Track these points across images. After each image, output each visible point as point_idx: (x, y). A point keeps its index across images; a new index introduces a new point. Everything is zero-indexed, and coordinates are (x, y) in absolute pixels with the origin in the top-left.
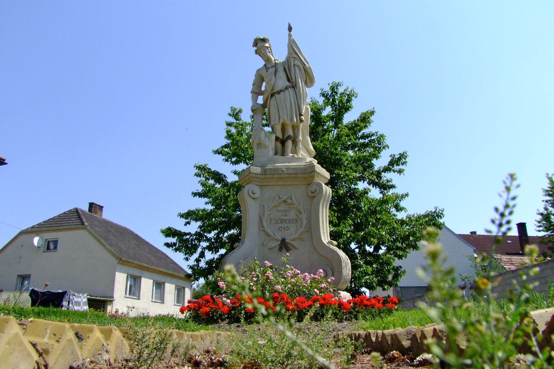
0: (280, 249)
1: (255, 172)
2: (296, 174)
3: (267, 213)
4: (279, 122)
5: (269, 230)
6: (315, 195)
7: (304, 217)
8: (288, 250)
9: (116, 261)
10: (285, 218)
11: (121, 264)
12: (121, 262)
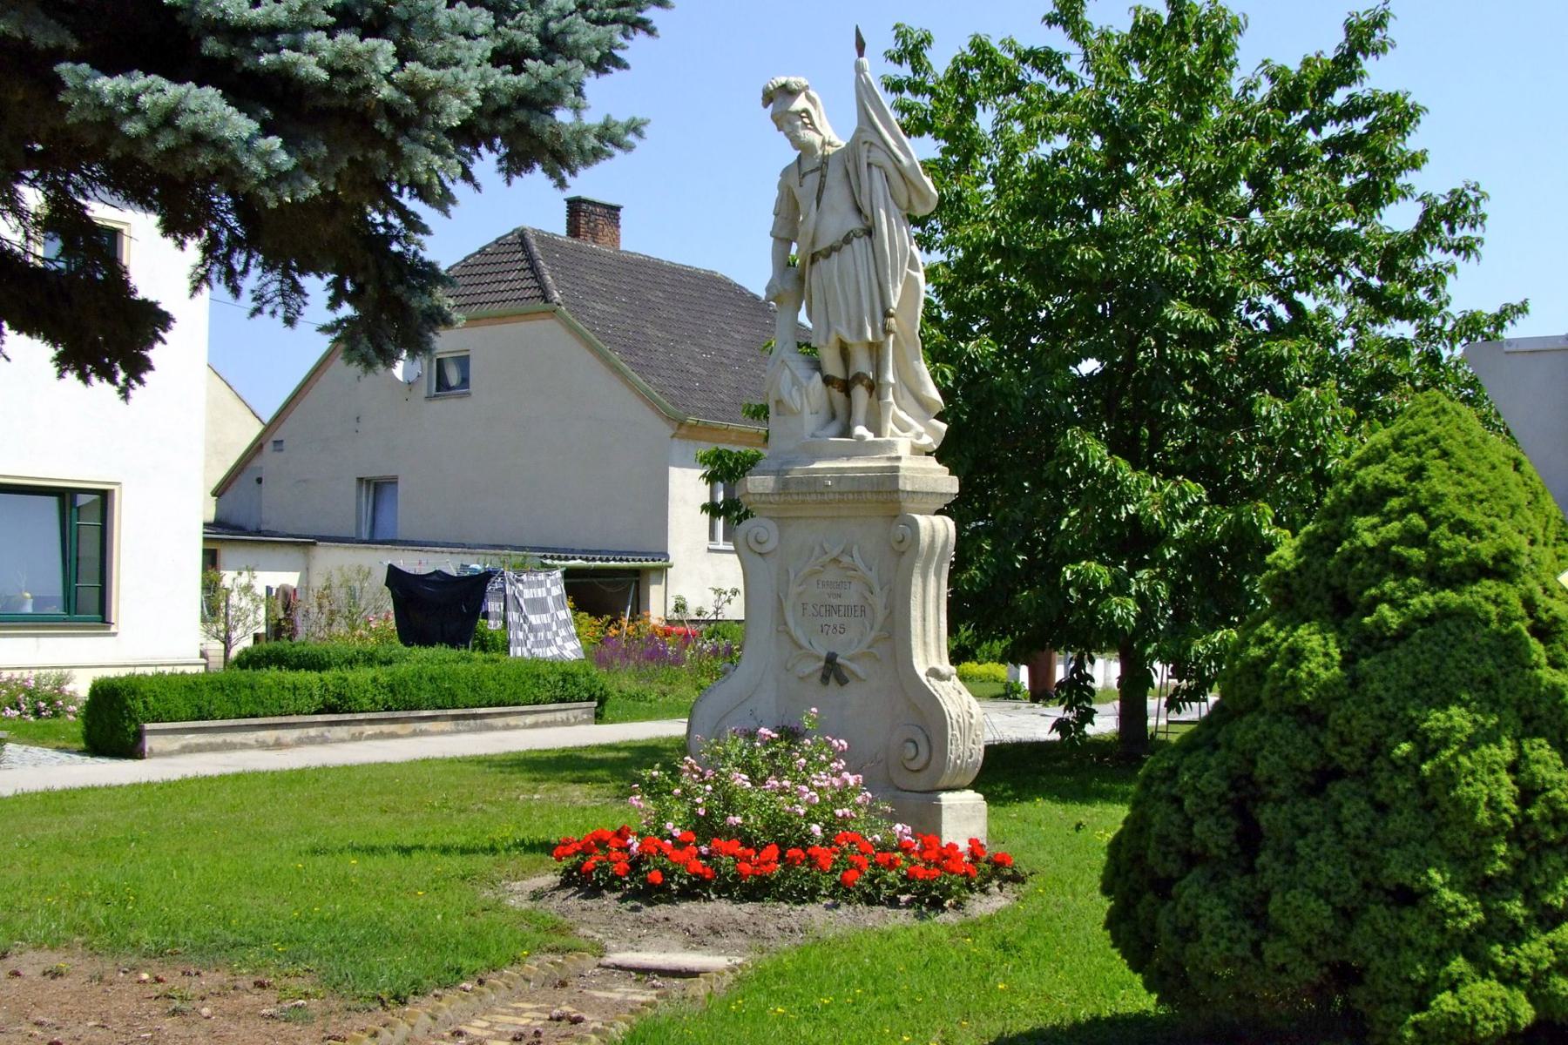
0: (825, 679)
1: (761, 490)
2: (859, 493)
3: (794, 589)
4: (827, 341)
5: (798, 633)
6: (904, 547)
7: (879, 601)
8: (842, 681)
9: (667, 430)
10: (835, 602)
11: (683, 437)
12: (683, 431)
